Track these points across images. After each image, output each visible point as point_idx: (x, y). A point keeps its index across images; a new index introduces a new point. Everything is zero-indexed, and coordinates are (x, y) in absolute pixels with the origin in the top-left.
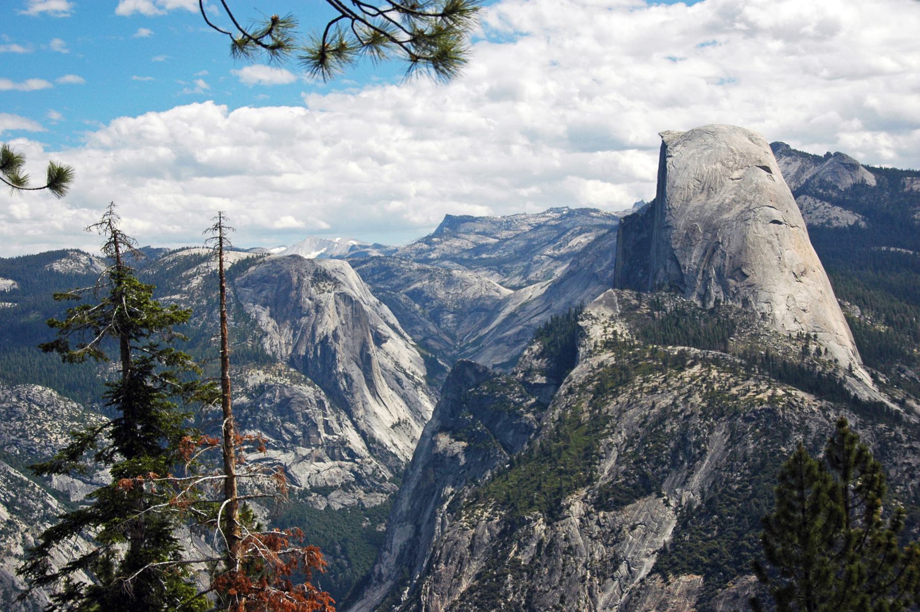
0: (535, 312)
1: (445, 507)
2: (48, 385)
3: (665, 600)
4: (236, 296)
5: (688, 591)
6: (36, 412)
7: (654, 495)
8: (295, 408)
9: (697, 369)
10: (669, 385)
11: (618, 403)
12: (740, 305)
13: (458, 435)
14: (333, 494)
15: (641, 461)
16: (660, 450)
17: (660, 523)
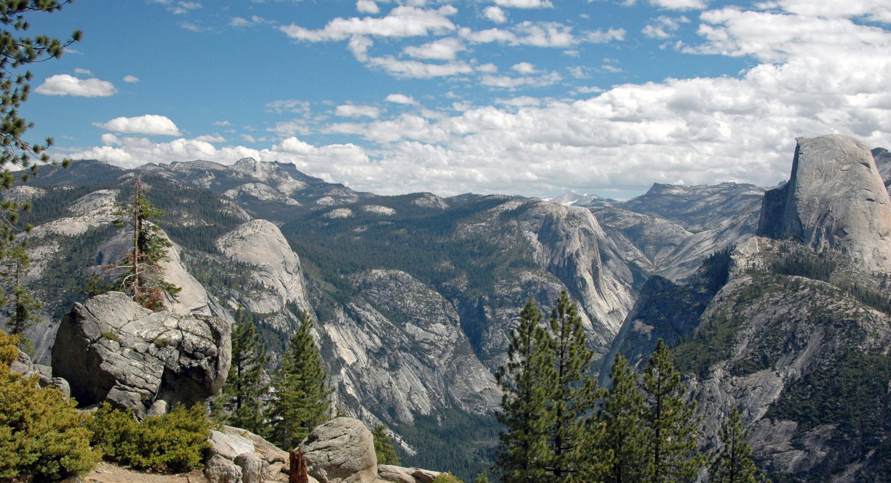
0: (707, 248)
2: (408, 271)
3: (770, 435)
4: (519, 226)
5: (787, 431)
7: (770, 369)
8: (550, 297)
9: (806, 291)
12: (840, 252)
13: (648, 322)
15: (764, 347)
16: (777, 341)
17: (773, 387)
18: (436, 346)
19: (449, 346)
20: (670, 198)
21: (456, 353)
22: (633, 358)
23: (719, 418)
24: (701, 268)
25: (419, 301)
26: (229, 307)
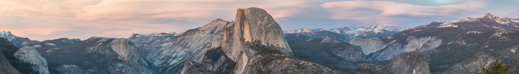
6: (75, 71)
9: (287, 59)
10: (283, 62)
20: (139, 38)
24: (204, 56)
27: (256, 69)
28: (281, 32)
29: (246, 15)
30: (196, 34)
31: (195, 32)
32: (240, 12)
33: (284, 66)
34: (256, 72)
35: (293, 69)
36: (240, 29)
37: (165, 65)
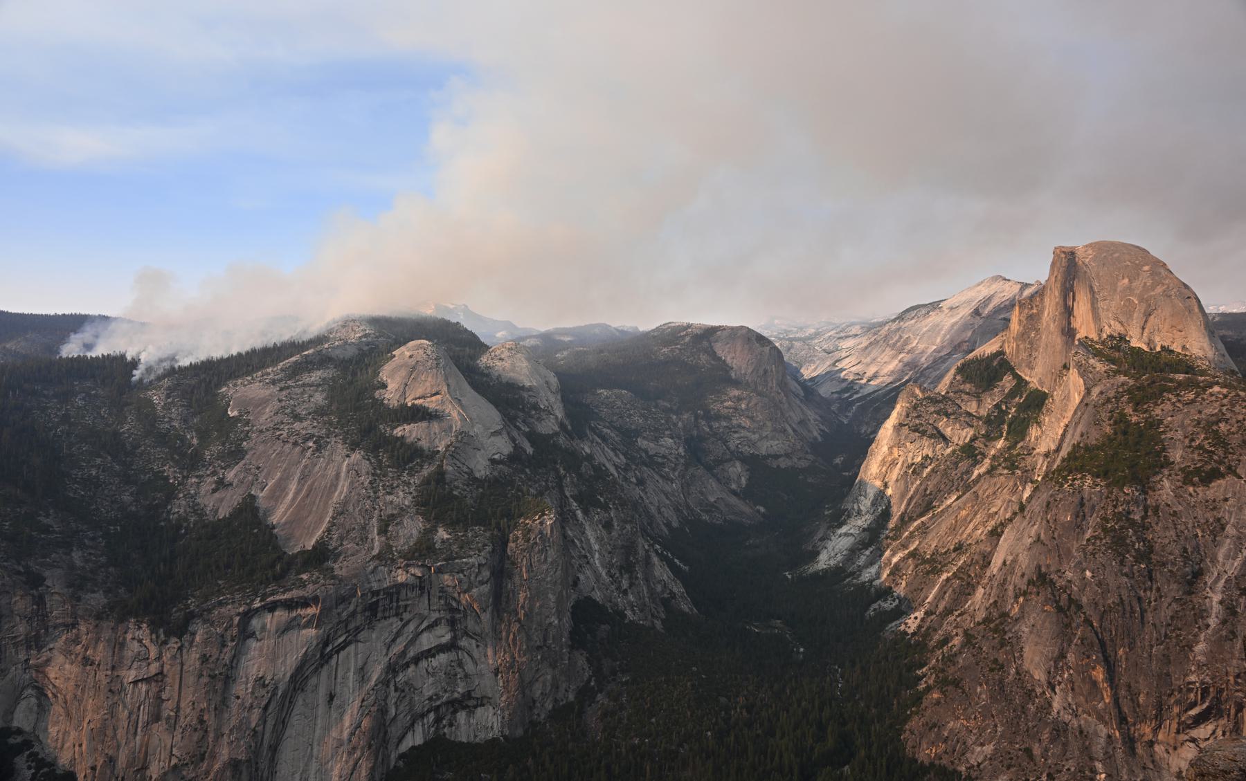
1: (910, 471)
6: (626, 405)
9: (1216, 389)
10: (1203, 399)
11: (1163, 410)
14: (781, 459)
15: (1211, 451)
18: (668, 459)
19: (680, 459)
21: (687, 466)
22: (902, 465)
23: (1198, 537)
24: (955, 375)
25: (646, 419)
26: (519, 429)
27: (1112, 416)
28: (1197, 310)
29: (1080, 262)
30: (934, 318)
31: (929, 312)
32: (1063, 256)
33: (1209, 411)
34: (1112, 422)
35: (1238, 422)
36: (1061, 302)
37: (846, 395)
